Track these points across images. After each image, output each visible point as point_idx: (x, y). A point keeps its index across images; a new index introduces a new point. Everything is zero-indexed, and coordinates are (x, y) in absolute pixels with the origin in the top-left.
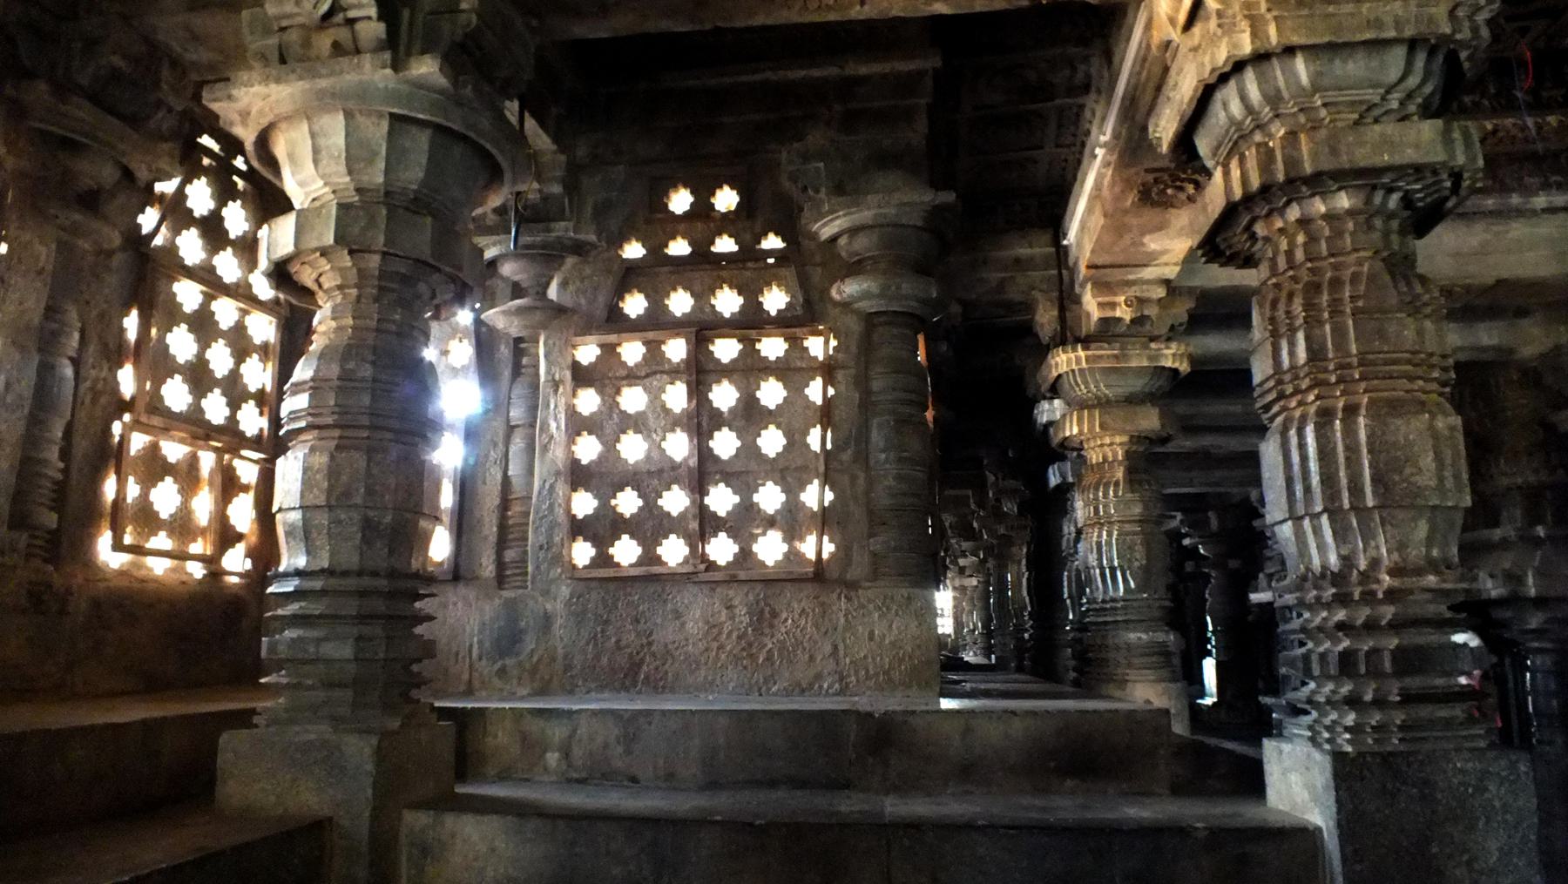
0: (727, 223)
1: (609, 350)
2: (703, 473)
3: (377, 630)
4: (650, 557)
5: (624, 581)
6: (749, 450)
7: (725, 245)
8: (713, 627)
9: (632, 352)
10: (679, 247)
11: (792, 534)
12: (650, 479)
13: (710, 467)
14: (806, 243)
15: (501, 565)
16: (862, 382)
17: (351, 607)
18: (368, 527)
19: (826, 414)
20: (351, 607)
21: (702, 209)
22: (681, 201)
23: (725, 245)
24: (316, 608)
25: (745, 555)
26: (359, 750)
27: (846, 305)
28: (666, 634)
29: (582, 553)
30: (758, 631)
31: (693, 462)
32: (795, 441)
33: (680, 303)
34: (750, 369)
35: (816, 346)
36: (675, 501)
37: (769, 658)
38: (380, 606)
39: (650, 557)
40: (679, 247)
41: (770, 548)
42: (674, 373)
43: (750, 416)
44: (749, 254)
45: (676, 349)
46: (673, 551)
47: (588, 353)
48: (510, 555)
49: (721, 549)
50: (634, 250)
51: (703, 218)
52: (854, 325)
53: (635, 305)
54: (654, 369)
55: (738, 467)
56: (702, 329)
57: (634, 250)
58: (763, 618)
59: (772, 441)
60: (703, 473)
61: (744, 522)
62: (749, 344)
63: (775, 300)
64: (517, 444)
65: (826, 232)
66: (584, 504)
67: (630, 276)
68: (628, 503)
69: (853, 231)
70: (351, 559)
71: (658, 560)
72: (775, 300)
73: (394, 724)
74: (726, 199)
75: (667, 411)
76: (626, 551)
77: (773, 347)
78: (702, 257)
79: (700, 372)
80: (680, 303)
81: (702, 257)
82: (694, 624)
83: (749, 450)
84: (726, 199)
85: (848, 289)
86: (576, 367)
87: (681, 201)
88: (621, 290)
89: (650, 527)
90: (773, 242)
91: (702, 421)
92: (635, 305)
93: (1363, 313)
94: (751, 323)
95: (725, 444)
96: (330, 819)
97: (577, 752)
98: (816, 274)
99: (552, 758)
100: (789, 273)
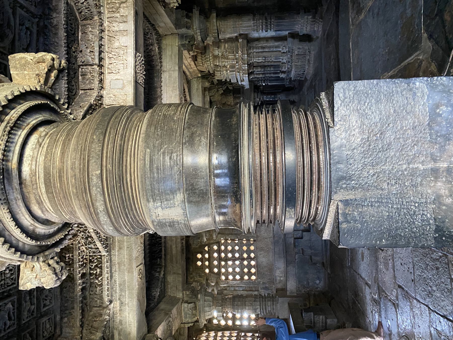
0: (203, 256)
1: (223, 274)
2: (242, 259)
3: (267, 300)
4: (254, 267)
5: (257, 271)
6: (238, 251)
7: (207, 256)
9: (223, 270)
10: (207, 263)
12: (242, 266)
13: (240, 258)
14: (207, 243)
15: (256, 291)
16: (228, 234)
17: (264, 302)
18: (254, 301)
19: (233, 240)
20: (264, 302)
21: (201, 260)
22: (199, 263)
23: (207, 256)
24: (264, 307)
26: (281, 300)
27: (217, 237)
28: (265, 264)
29: (253, 277)
30: (264, 250)
31: (240, 260)
32: (237, 244)
33: (216, 263)
34: (226, 251)
35: (223, 241)
36: (245, 263)
37: (268, 248)
38: (264, 300)
39: (254, 267)
40: (207, 263)
42: (226, 263)
43: (233, 251)
44: (208, 252)
45: (223, 263)
46: (253, 263)
47: (223, 278)
48: (254, 289)
49: (252, 255)
51: (202, 260)
52: (219, 235)
53: (216, 270)
54: (226, 267)
55: (240, 253)
56: (220, 259)
57: (207, 271)
58: (262, 249)
60: (242, 259)
61: (249, 252)
62: (223, 251)
63: (215, 247)
64: (237, 289)
65: (205, 240)
66: (246, 277)
67: (211, 271)
68: (246, 270)
69: (206, 236)
70: (258, 303)
71: (254, 265)
72: (215, 247)
73: (277, 297)
74: (199, 256)
75: (232, 264)
77: (223, 248)
78: (209, 260)
79: (226, 259)
80: (216, 263)
81: (209, 260)
82: (264, 260)
83: (238, 251)
84: (199, 256)
85: (214, 236)
86: (225, 279)
87: (199, 263)
88: (214, 273)
90: (206, 248)
92: (216, 270)
93: (159, 48)
94: (219, 251)
95: (237, 255)
96: (289, 304)
97: (281, 275)
98: (212, 242)
99: (282, 279)
100: (211, 246)
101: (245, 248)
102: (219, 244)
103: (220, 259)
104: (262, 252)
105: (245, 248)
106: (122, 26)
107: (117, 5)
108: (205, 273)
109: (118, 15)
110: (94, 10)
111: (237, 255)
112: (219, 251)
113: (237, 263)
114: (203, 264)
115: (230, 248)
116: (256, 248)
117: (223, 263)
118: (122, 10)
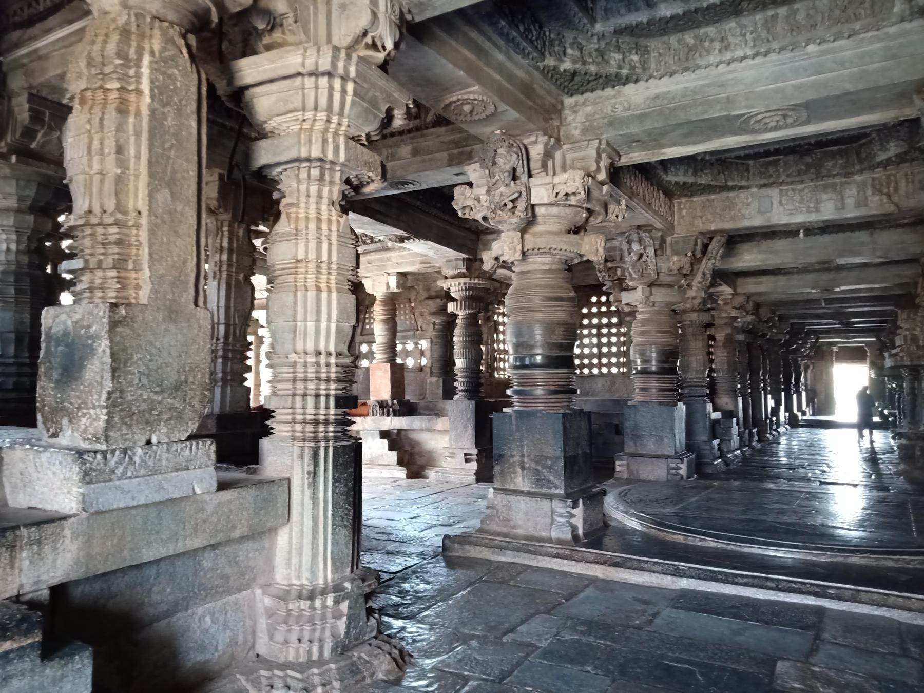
2: (600, 355)
8: (603, 386)
11: (618, 367)
12: (591, 356)
22: (594, 299)
25: (609, 371)
35: (622, 330)
36: (595, 361)
41: (614, 370)
50: (585, 311)
58: (613, 383)
59: (614, 349)
60: (600, 355)
68: (586, 361)
76: (586, 371)
77: (614, 330)
79: (599, 335)
80: (595, 321)
89: (591, 366)
91: (600, 345)
92: (586, 322)
95: (605, 350)
101: (614, 360)
102: (618, 325)
103: (599, 327)
104: (609, 383)
105: (614, 360)
106: (850, 202)
107: (885, 191)
108: (582, 308)
109: (869, 192)
110: (866, 165)
111: (605, 350)
112: (609, 325)
113: (595, 350)
114: (593, 305)
115: (614, 339)
116: (613, 375)
117: (594, 331)
118: (877, 198)
